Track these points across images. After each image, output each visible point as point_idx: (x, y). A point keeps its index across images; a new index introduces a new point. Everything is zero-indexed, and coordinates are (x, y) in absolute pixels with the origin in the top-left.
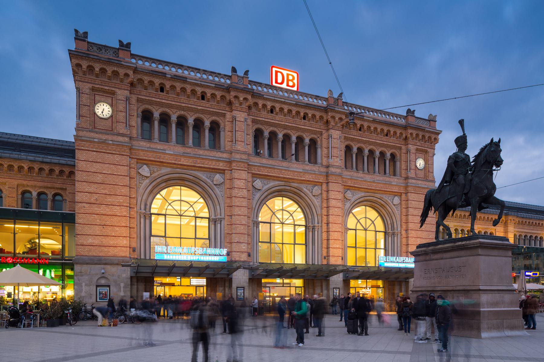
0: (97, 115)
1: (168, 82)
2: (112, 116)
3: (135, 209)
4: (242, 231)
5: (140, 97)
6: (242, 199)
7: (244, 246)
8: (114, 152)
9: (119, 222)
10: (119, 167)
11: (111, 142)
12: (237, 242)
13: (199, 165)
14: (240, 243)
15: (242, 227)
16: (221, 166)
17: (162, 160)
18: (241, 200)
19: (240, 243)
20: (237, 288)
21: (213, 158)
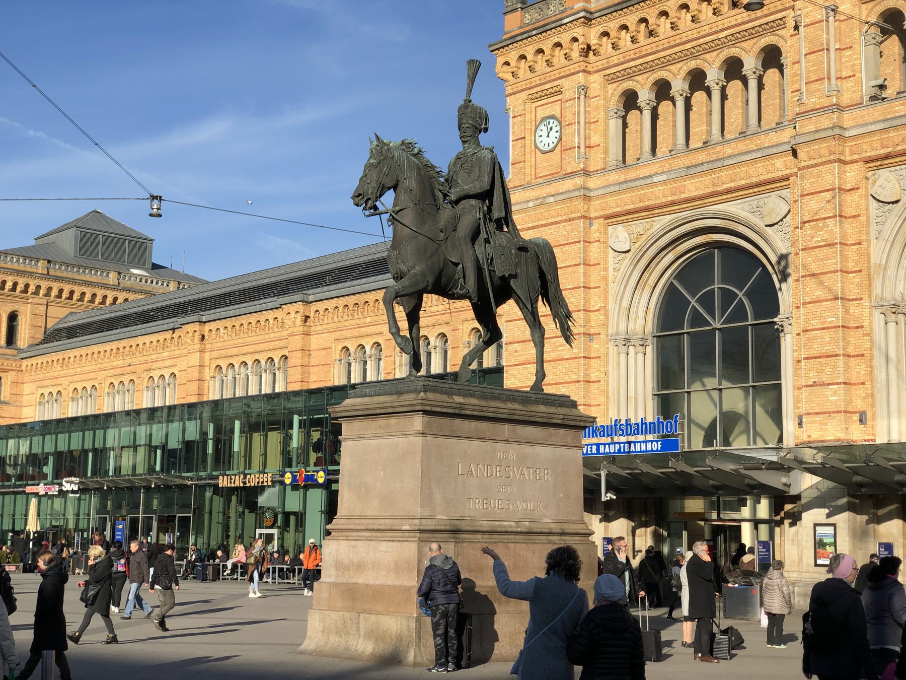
0: (539, 149)
1: (652, 10)
2: (560, 139)
3: (603, 336)
4: (828, 349)
5: (608, 72)
6: (826, 250)
7: (835, 393)
8: (558, 219)
9: (567, 373)
10: (567, 248)
11: (551, 199)
12: (815, 384)
13: (725, 186)
14: (823, 384)
15: (827, 336)
16: (781, 166)
17: (647, 203)
18: (821, 256)
19: (823, 384)
20: (816, 525)
21: (754, 156)
